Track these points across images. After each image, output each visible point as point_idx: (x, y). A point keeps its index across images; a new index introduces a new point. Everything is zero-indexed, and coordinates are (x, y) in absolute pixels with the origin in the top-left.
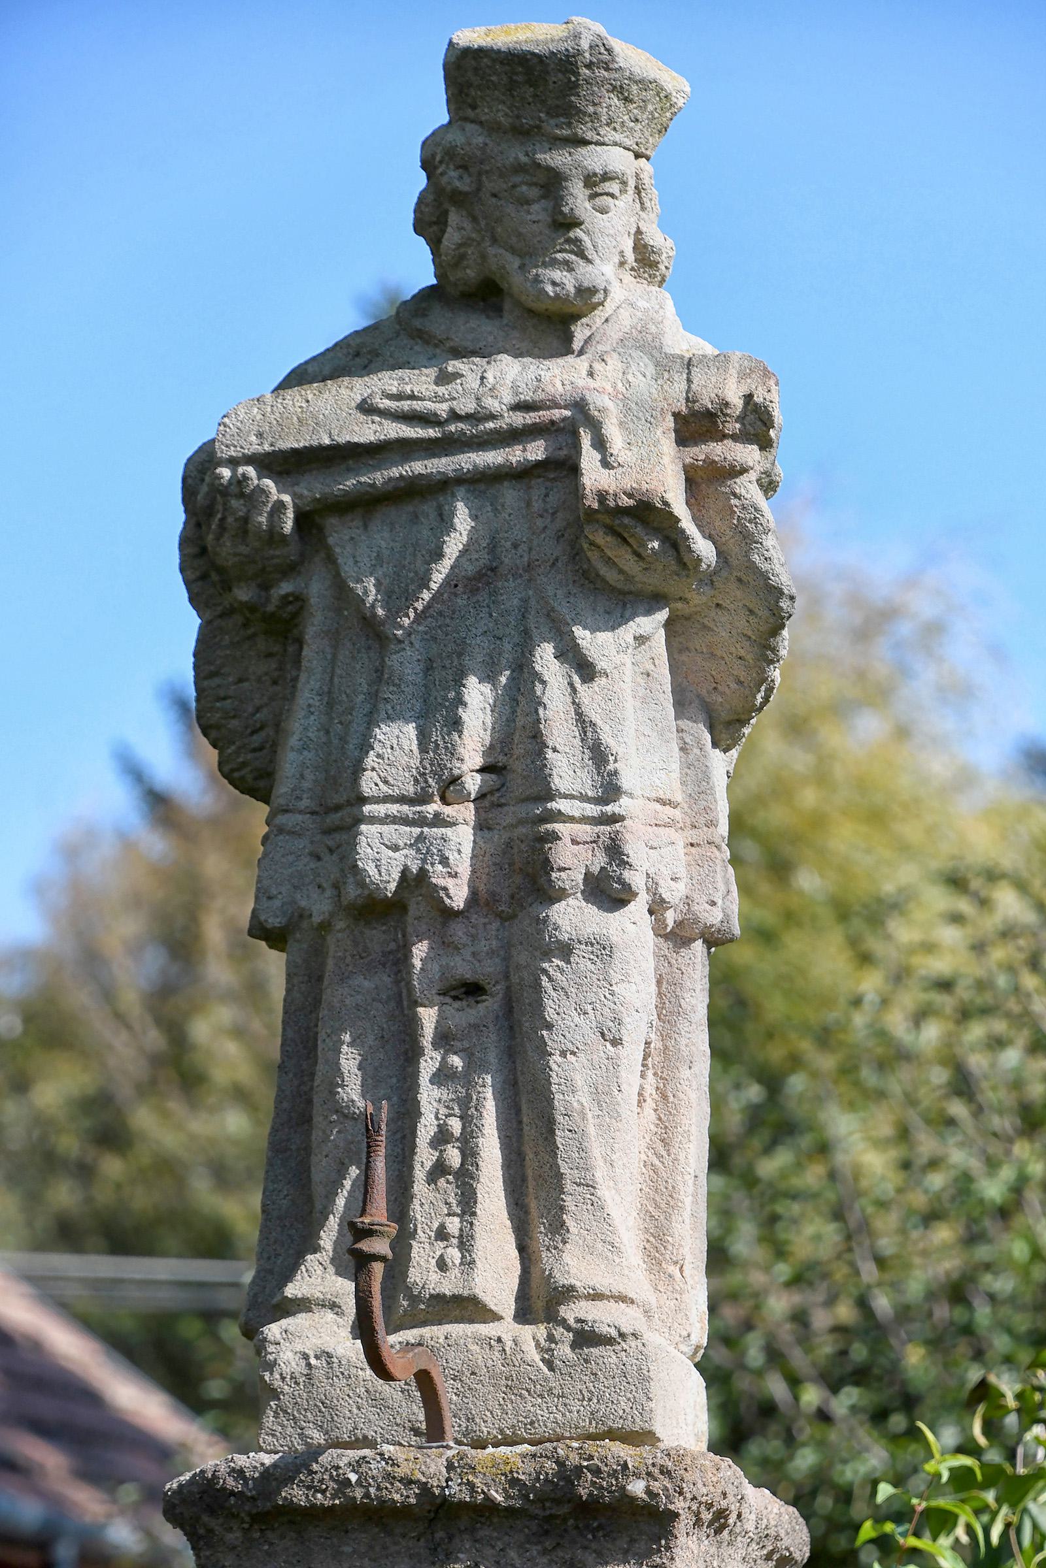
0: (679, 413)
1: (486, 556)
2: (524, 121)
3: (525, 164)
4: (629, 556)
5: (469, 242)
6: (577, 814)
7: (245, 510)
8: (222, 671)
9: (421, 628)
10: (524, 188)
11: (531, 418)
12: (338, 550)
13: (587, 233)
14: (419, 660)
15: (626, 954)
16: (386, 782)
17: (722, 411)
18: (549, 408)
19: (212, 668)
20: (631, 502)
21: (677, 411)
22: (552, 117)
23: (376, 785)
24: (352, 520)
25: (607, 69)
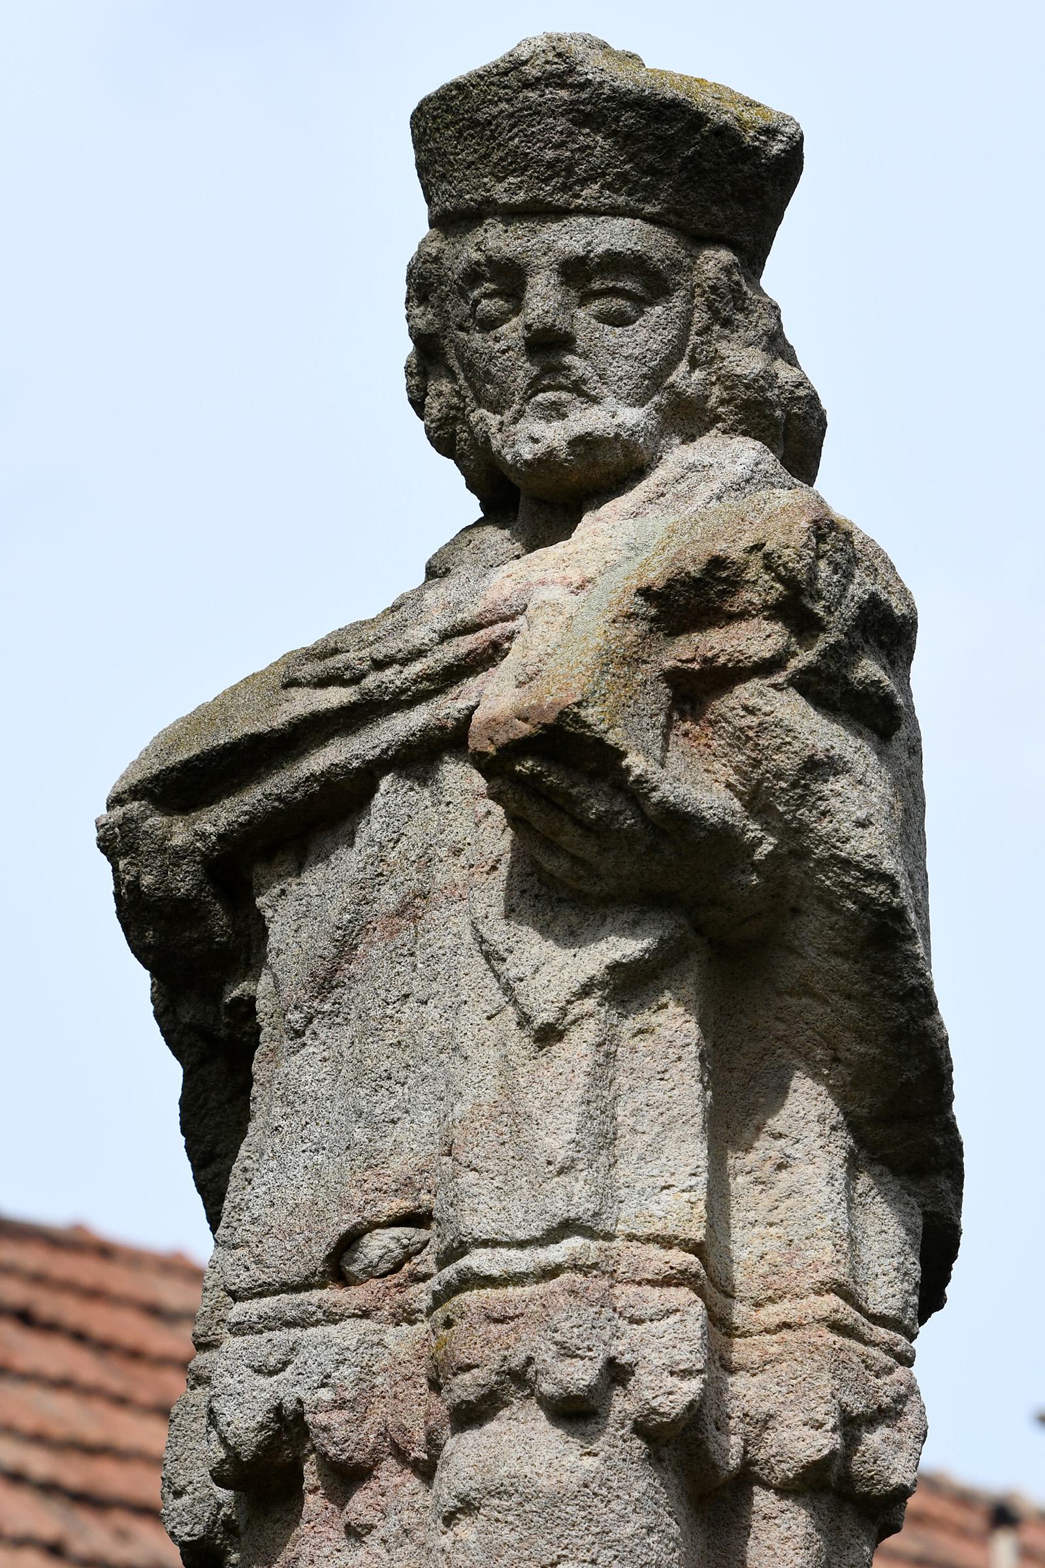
0: (649, 588)
1: (415, 876)
2: (467, 197)
3: (478, 263)
4: (569, 827)
5: (453, 412)
6: (496, 1272)
7: (133, 870)
8: (218, 1150)
9: (327, 1007)
10: (484, 302)
11: (465, 644)
12: (269, 913)
13: (585, 356)
14: (325, 1060)
15: (569, 1509)
16: (258, 1261)
17: (713, 577)
18: (492, 623)
19: (202, 1148)
20: (525, 728)
21: (644, 585)
22: (500, 180)
23: (247, 1269)
24: (281, 863)
25: (562, 86)
